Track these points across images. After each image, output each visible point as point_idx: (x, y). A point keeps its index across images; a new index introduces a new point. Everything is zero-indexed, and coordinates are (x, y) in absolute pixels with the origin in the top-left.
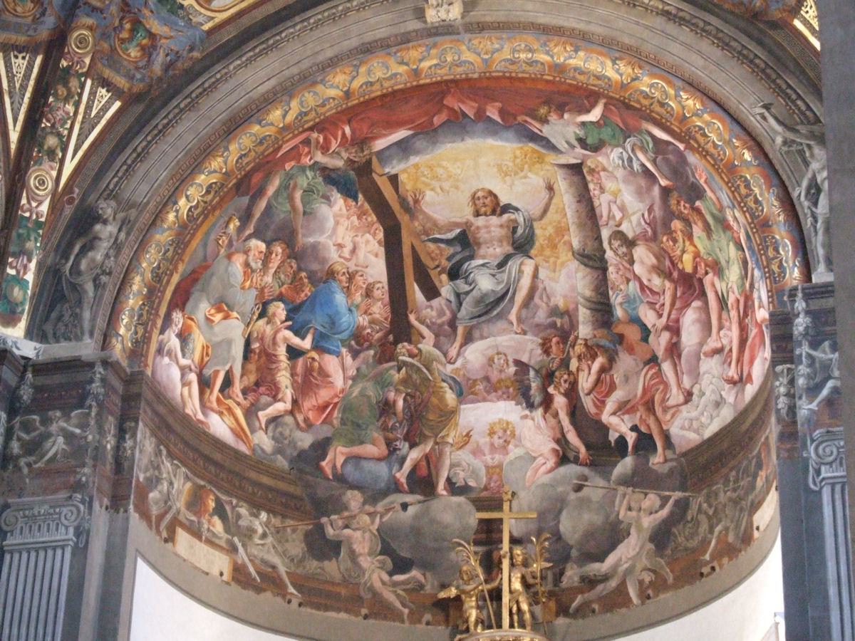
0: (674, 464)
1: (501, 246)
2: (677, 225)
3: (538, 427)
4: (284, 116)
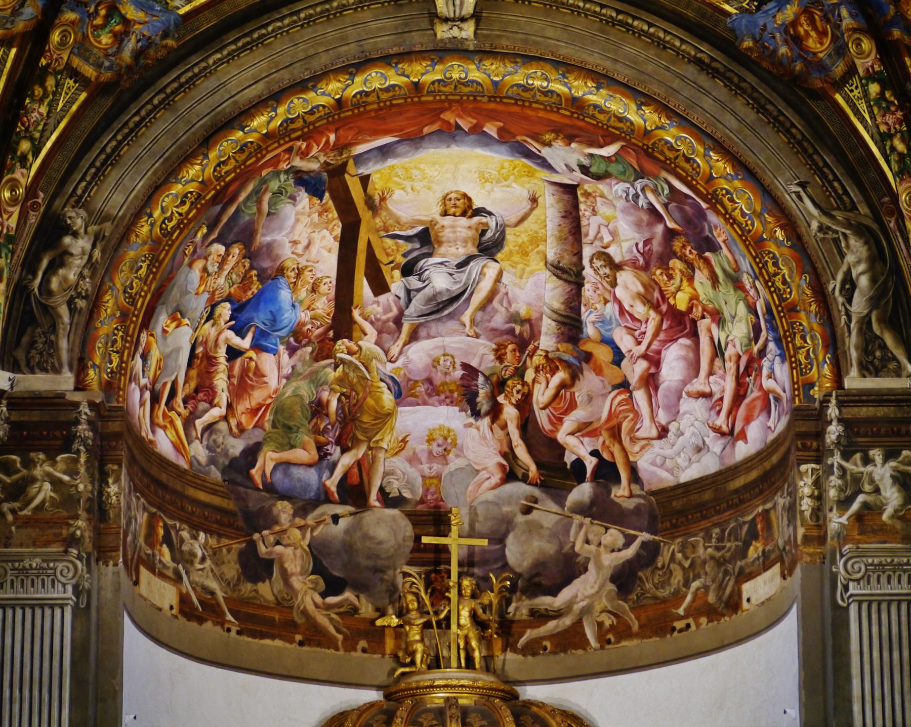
0: (642, 501)
1: (465, 247)
2: (676, 264)
3: (484, 438)
4: (269, 123)
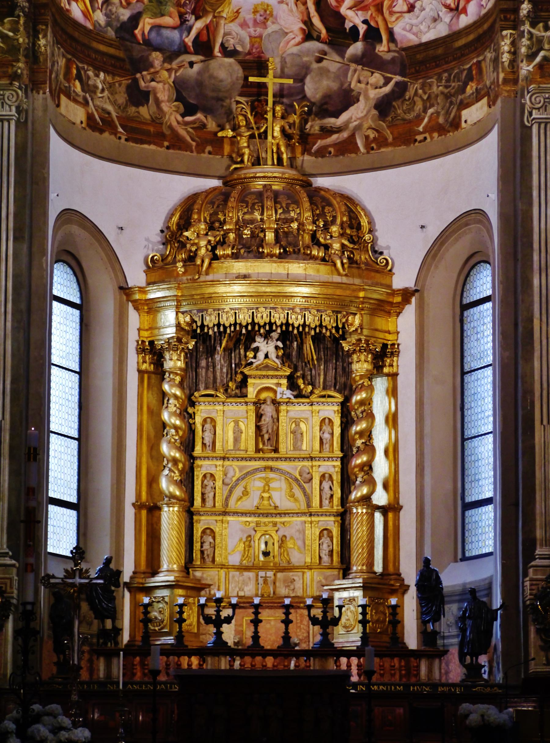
0: (396, 54)
